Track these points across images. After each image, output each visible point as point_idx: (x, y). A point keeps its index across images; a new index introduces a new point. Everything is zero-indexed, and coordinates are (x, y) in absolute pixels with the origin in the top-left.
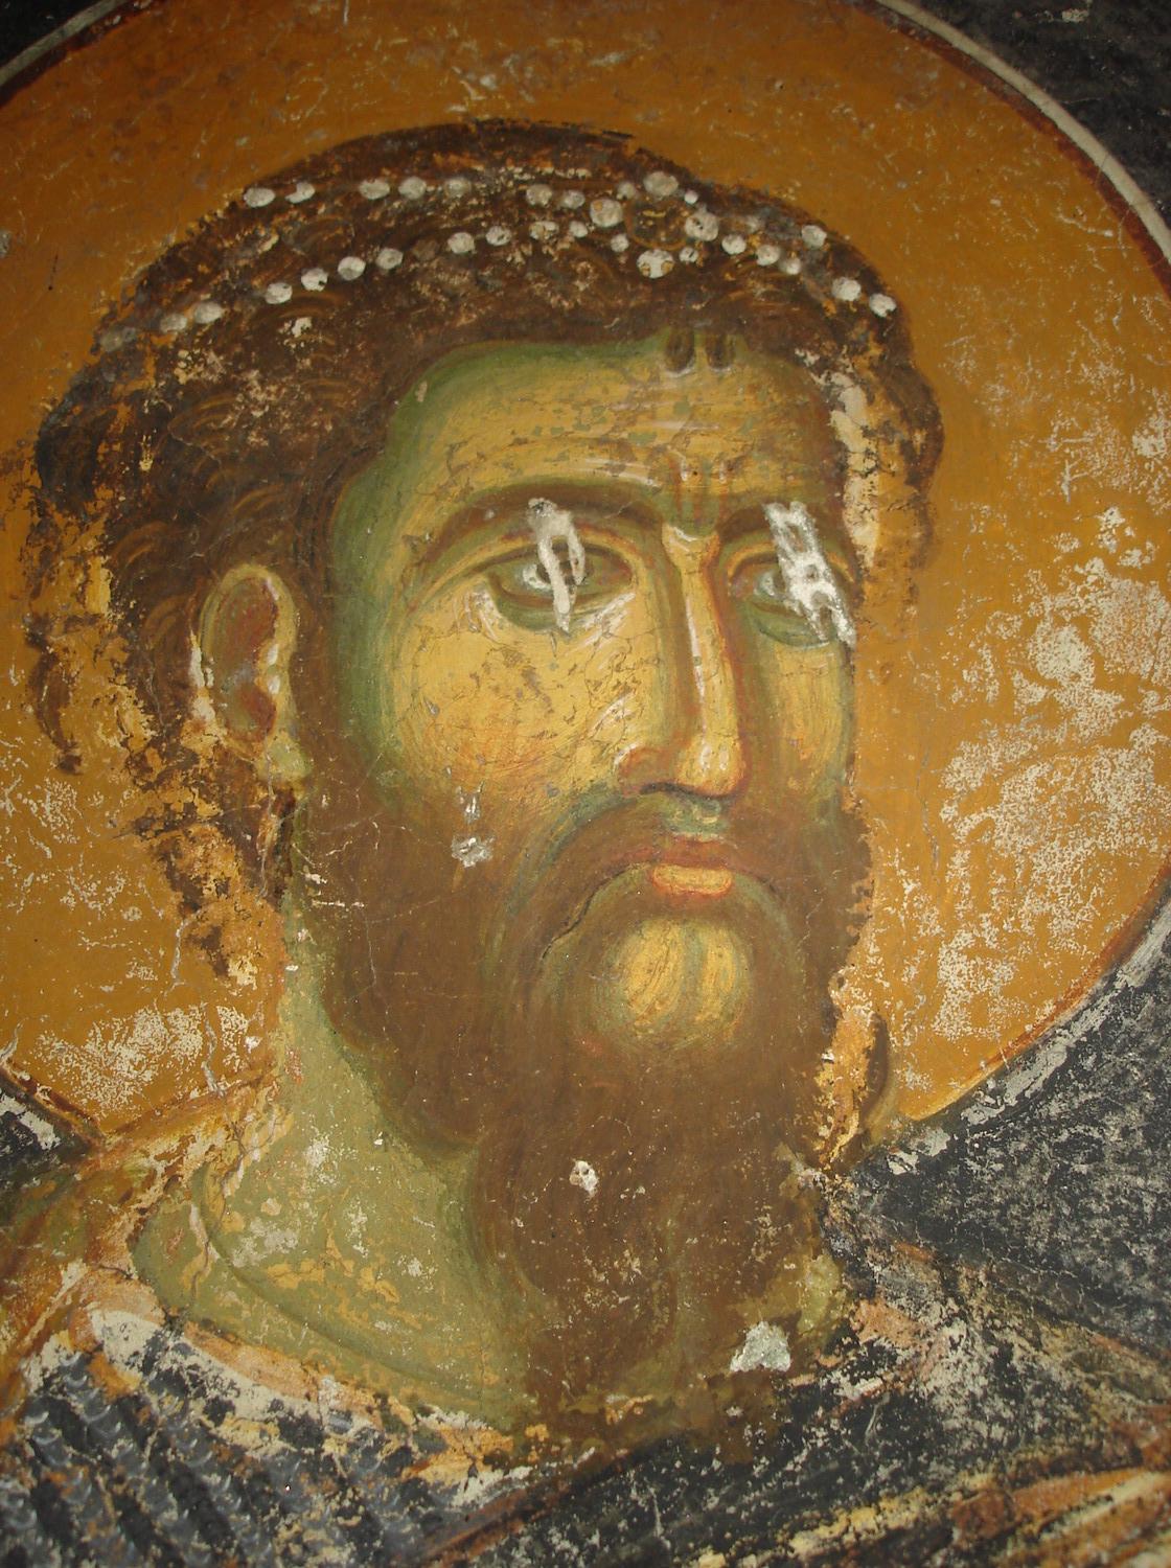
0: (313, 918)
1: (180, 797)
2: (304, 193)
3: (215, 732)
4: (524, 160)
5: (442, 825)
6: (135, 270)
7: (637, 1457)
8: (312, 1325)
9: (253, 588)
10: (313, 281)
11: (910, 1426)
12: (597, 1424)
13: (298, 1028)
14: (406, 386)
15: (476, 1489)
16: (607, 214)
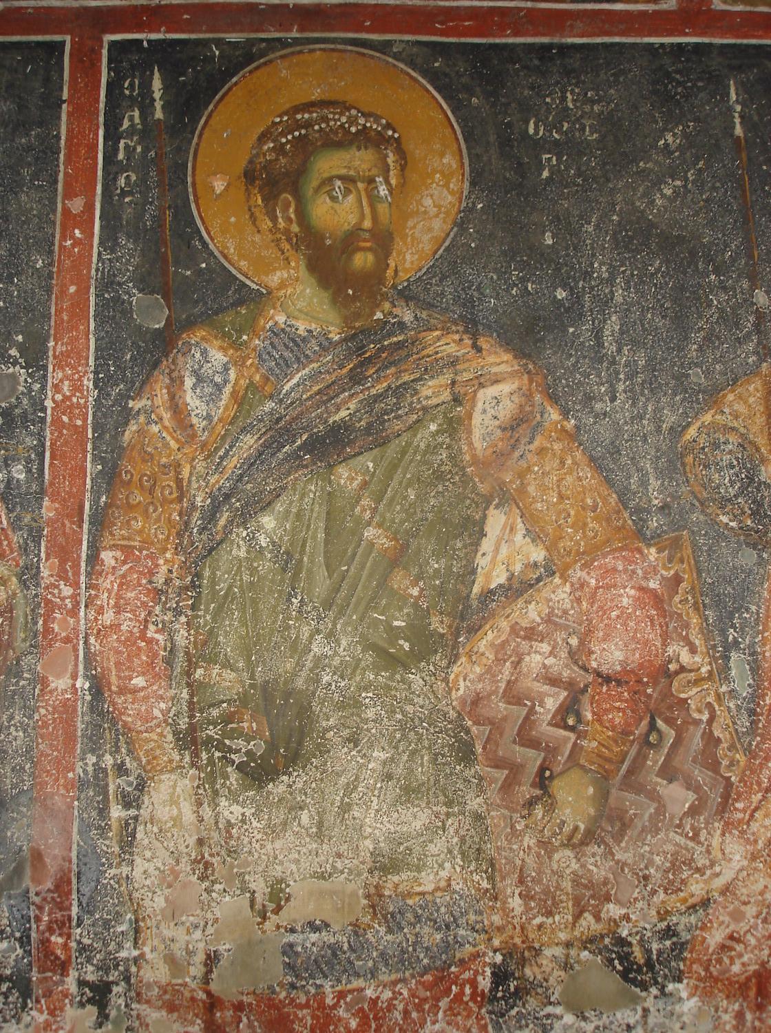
0: (303, 254)
1: (279, 236)
2: (285, 118)
3: (283, 224)
4: (327, 108)
5: (323, 238)
6: (255, 137)
7: (361, 332)
8: (309, 315)
9: (286, 199)
10: (290, 137)
11: (402, 325)
12: (352, 328)
13: (303, 272)
14: (309, 158)
15: (337, 338)
16: (344, 119)
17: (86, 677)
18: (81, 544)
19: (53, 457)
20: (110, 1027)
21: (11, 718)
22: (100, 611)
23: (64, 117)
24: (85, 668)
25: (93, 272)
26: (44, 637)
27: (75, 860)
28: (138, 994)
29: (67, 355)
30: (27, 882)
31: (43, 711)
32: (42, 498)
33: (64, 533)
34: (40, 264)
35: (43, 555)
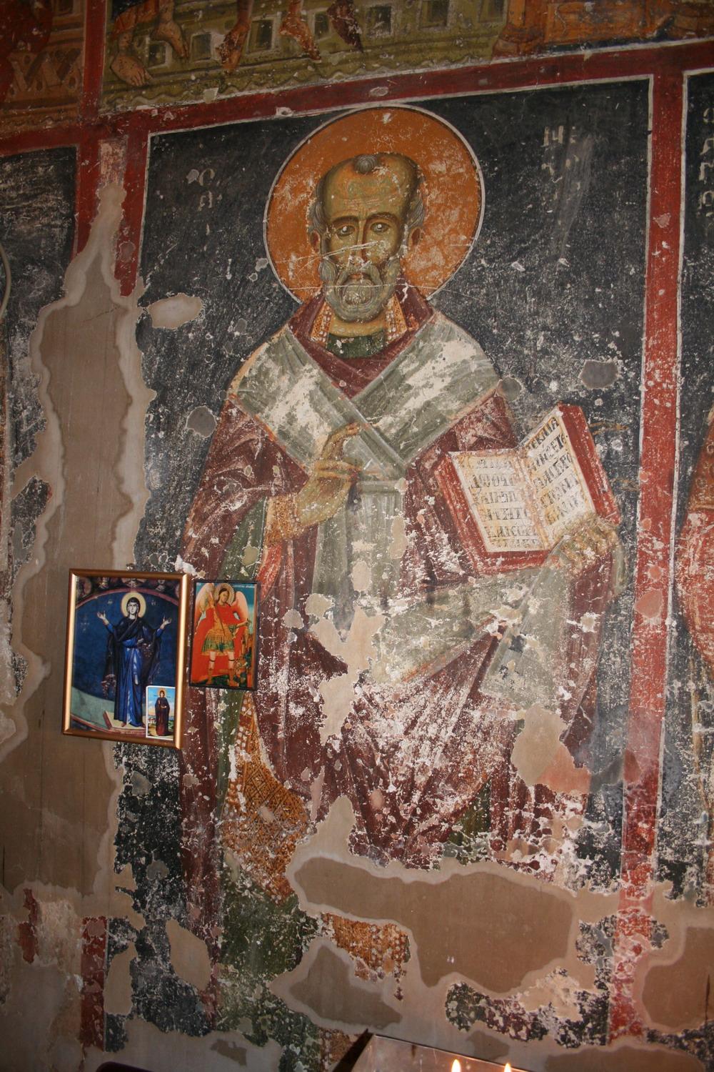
17: (674, 617)
18: (671, 507)
19: (646, 433)
20: (683, 899)
21: (611, 646)
22: (687, 563)
23: (650, 146)
24: (674, 609)
25: (679, 278)
26: (639, 582)
27: (661, 764)
28: (709, 876)
29: (658, 347)
30: (621, 778)
31: (637, 643)
32: (637, 468)
33: (657, 497)
34: (632, 272)
35: (639, 515)
